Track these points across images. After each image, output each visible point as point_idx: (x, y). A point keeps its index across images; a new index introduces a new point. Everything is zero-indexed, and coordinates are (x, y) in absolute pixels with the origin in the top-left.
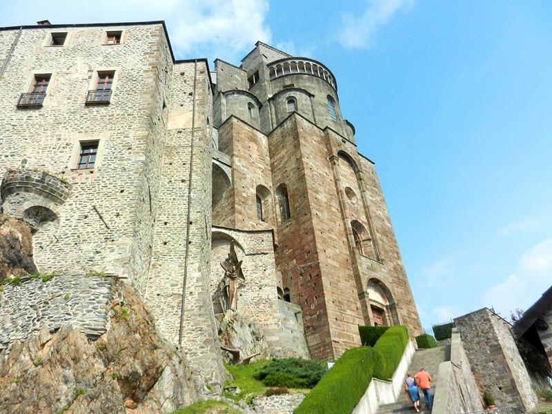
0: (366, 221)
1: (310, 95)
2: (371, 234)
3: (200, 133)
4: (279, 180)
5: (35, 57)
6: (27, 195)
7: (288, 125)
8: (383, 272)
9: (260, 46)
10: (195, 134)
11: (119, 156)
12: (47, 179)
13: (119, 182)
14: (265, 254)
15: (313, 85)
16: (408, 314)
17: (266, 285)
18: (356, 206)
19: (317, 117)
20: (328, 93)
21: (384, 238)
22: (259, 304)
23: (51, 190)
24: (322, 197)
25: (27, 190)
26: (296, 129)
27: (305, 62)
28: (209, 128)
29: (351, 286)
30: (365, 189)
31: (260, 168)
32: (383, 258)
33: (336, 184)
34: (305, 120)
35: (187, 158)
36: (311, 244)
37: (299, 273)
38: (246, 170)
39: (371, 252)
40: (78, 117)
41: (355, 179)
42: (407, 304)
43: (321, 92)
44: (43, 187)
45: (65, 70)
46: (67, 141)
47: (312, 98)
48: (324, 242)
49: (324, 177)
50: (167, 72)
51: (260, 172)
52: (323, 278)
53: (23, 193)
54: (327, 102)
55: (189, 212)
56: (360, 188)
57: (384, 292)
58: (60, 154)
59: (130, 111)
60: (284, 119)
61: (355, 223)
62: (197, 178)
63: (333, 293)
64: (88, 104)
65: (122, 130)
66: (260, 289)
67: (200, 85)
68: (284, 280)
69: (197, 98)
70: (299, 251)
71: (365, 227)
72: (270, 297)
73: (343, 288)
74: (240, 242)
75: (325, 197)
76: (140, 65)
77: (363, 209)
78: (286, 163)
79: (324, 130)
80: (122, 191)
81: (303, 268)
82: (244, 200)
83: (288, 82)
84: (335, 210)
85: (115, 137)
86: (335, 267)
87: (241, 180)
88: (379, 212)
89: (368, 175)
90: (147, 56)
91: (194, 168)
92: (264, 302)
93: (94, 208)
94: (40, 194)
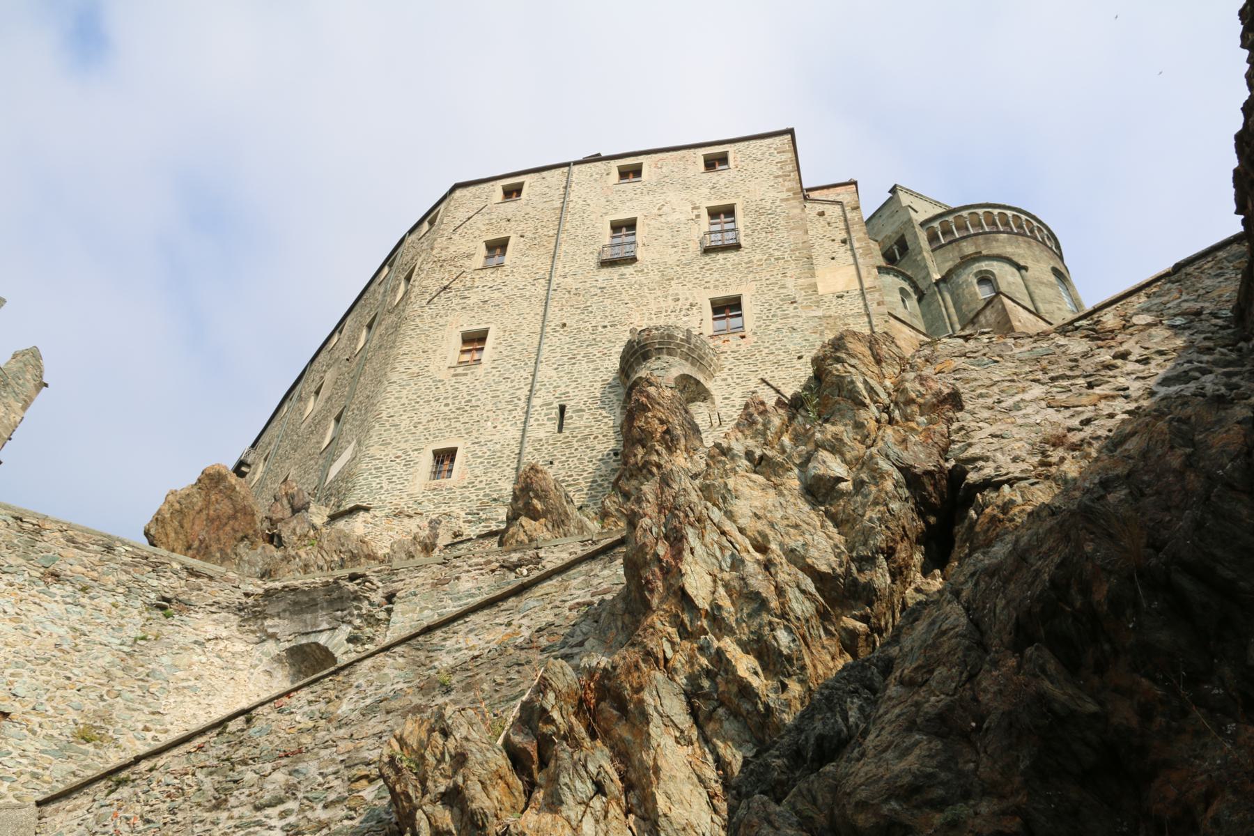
1: (1019, 268)
3: (876, 295)
5: (603, 200)
6: (670, 359)
7: (990, 315)
9: (900, 193)
10: (868, 297)
11: (779, 313)
12: (693, 340)
13: (791, 347)
15: (1021, 251)
20: (1053, 264)
23: (702, 358)
25: (669, 354)
26: (1008, 321)
27: (996, 211)
40: (696, 268)
44: (689, 349)
45: (656, 211)
46: (691, 301)
47: (1023, 272)
53: (665, 357)
54: (1053, 279)
58: (685, 319)
59: (777, 253)
60: (975, 312)
64: (707, 251)
65: (773, 280)
67: (856, 227)
69: (856, 245)
76: (772, 193)
80: (800, 358)
83: (969, 248)
85: (765, 290)
90: (780, 180)
93: (763, 381)
94: (687, 360)
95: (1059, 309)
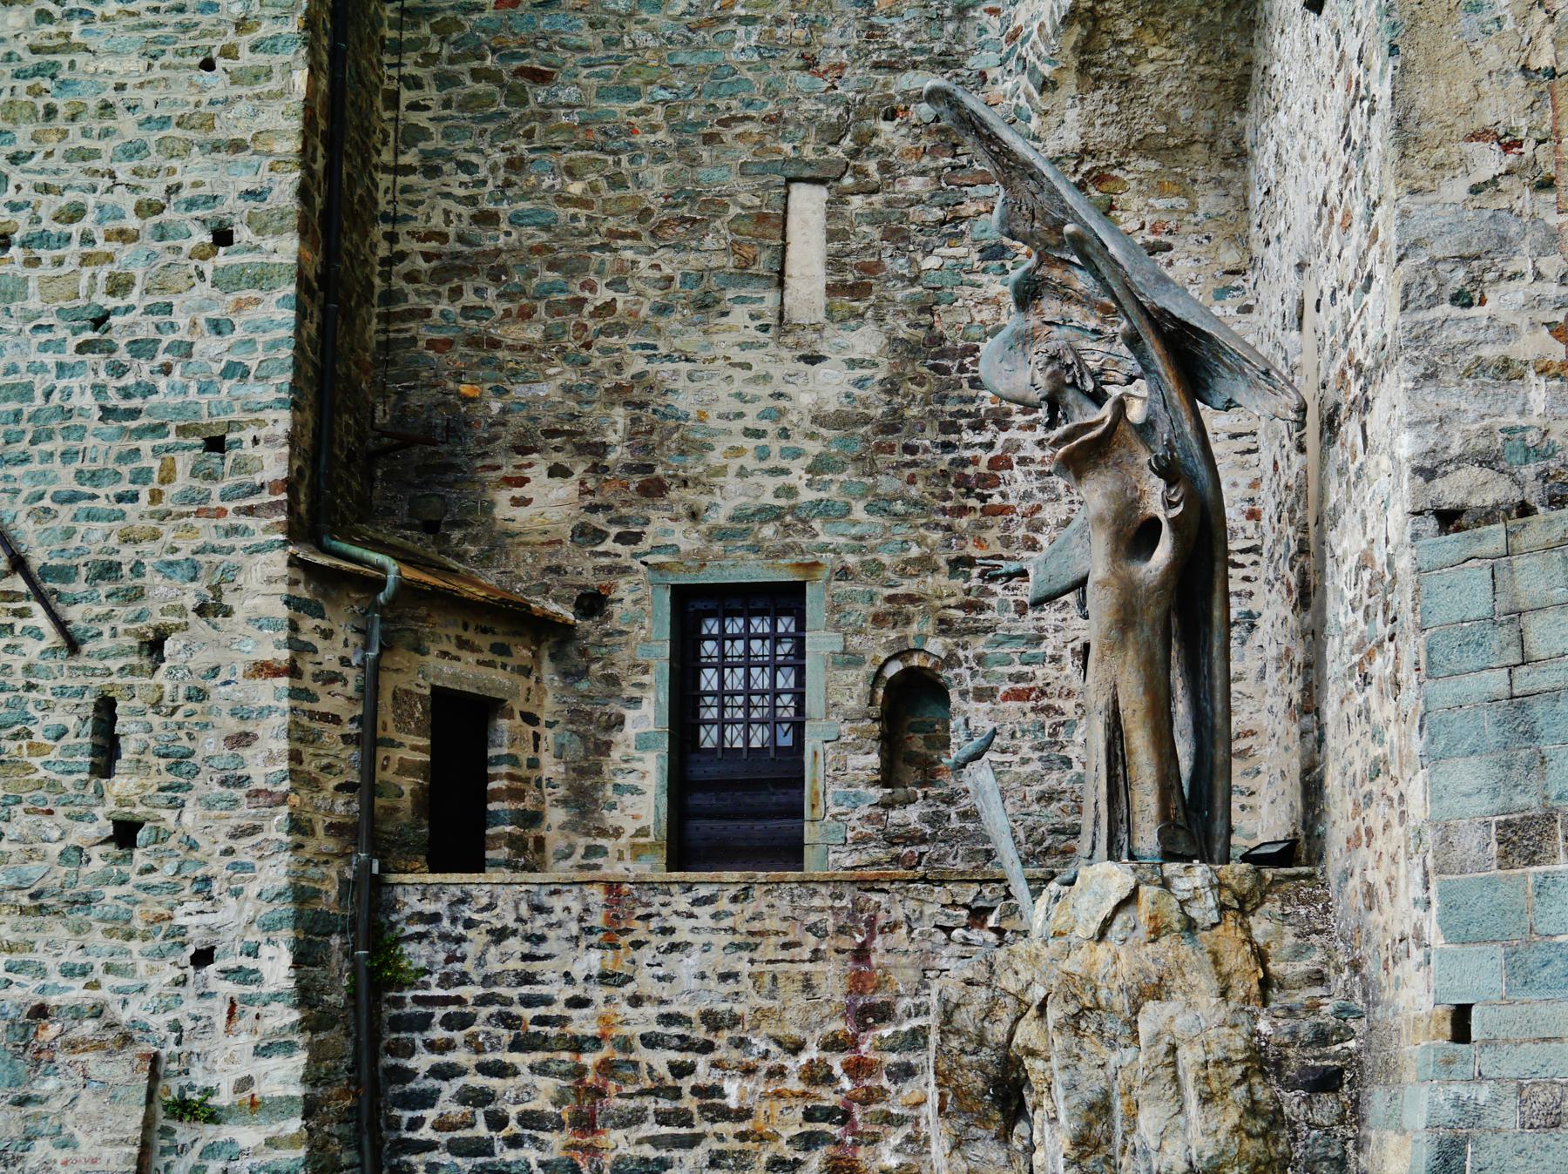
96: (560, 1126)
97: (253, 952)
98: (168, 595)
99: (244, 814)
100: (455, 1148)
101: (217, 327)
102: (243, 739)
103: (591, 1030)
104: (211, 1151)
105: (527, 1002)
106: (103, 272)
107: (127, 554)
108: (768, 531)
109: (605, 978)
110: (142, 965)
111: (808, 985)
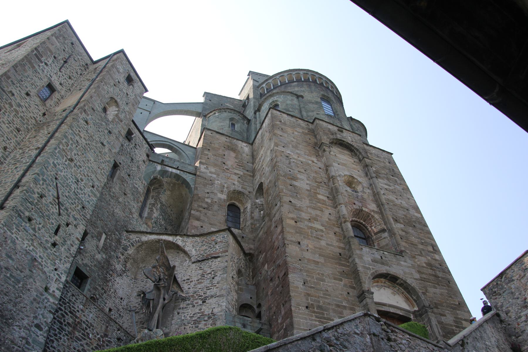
0: (376, 209)
1: (298, 97)
2: (385, 224)
4: (258, 182)
8: (401, 265)
14: (216, 258)
16: (455, 322)
17: (212, 296)
18: (360, 194)
19: (304, 114)
20: (322, 93)
21: (410, 230)
22: (199, 322)
24: (303, 183)
27: (294, 73)
28: (118, 111)
29: (345, 285)
30: (374, 175)
31: (235, 174)
32: (403, 249)
33: (327, 170)
34: (285, 116)
35: (53, 127)
36: (280, 237)
37: (269, 280)
38: (214, 176)
39: (387, 245)
41: (359, 167)
42: (454, 309)
43: (312, 92)
47: (300, 98)
48: (299, 231)
49: (309, 164)
50: (65, 62)
51: (236, 178)
52: (290, 276)
55: (23, 175)
56: (367, 175)
57: (409, 292)
61: (359, 213)
62: (55, 142)
63: (309, 295)
66: (204, 302)
68: (257, 294)
70: (269, 253)
71: (376, 216)
72: (215, 311)
73: (329, 289)
74: (187, 249)
75: (307, 184)
77: (371, 198)
78: (263, 161)
79: (312, 123)
81: (273, 270)
82: (206, 206)
84: (325, 198)
86: (317, 263)
87: (205, 185)
88: (400, 201)
89: (382, 165)
91: (57, 135)
92: (206, 318)
95: (317, 114)
96: (71, 327)
97: (62, 274)
98: (71, 220)
99: (68, 255)
100: (58, 321)
101: (89, 195)
102: (73, 246)
103: (78, 316)
104: (46, 298)
105: (73, 307)
106: (81, 177)
107: (70, 210)
108: (88, 268)
109: (82, 310)
110: (49, 264)
111: (101, 327)
